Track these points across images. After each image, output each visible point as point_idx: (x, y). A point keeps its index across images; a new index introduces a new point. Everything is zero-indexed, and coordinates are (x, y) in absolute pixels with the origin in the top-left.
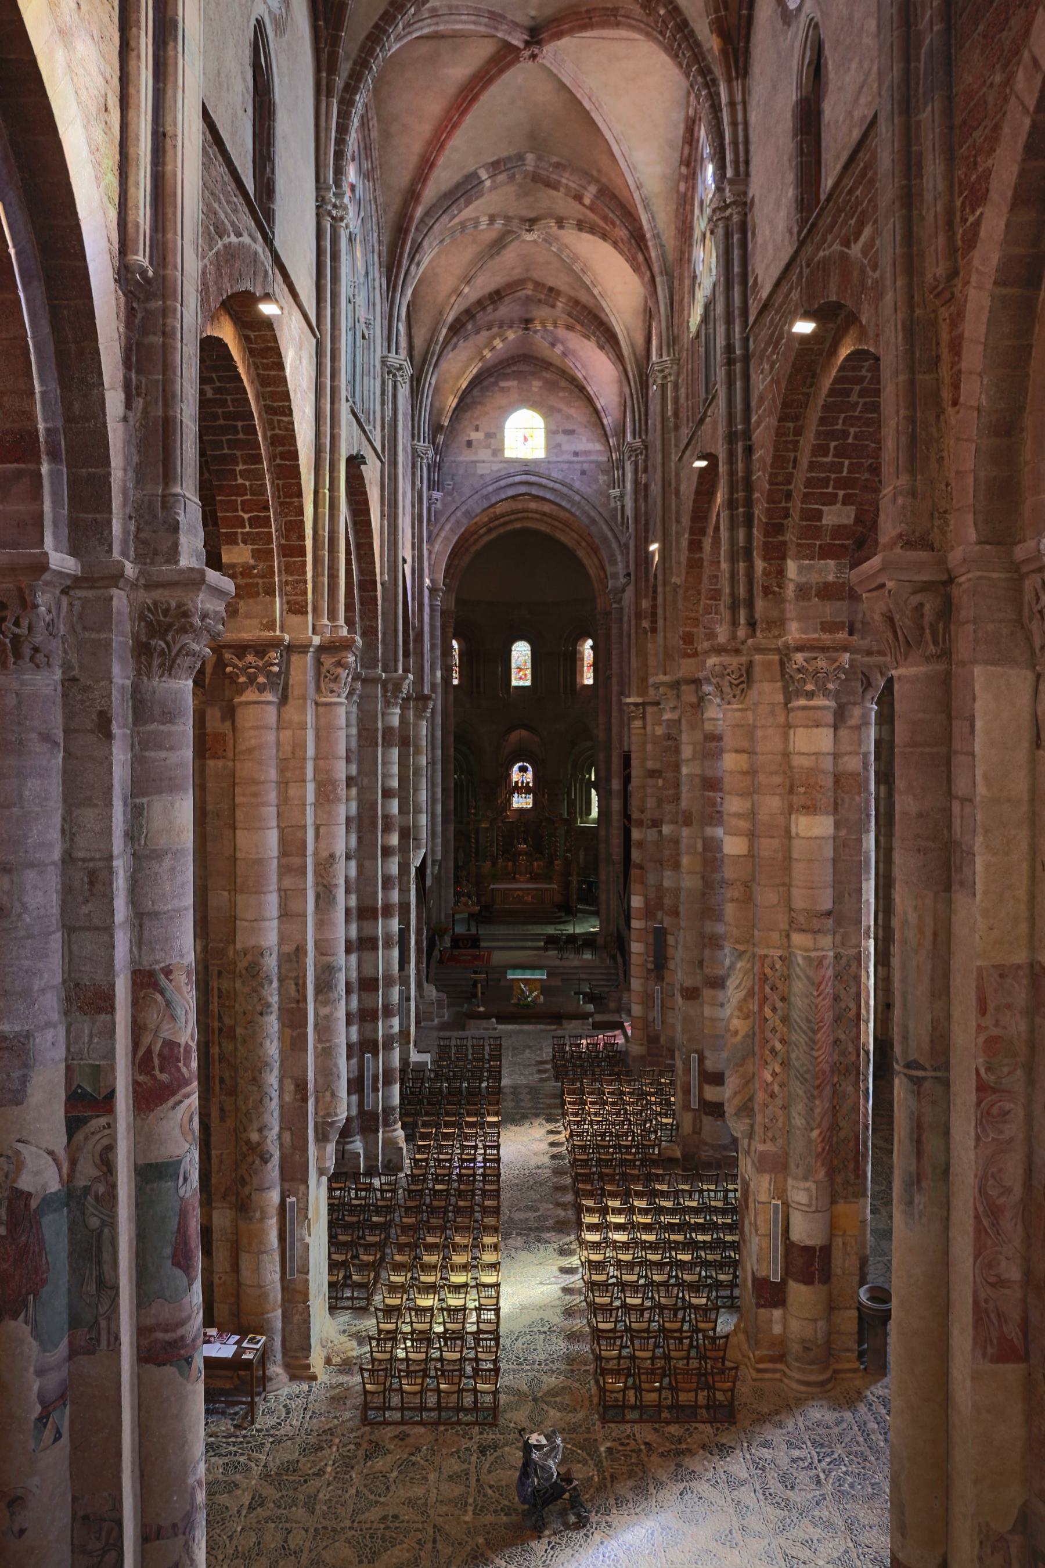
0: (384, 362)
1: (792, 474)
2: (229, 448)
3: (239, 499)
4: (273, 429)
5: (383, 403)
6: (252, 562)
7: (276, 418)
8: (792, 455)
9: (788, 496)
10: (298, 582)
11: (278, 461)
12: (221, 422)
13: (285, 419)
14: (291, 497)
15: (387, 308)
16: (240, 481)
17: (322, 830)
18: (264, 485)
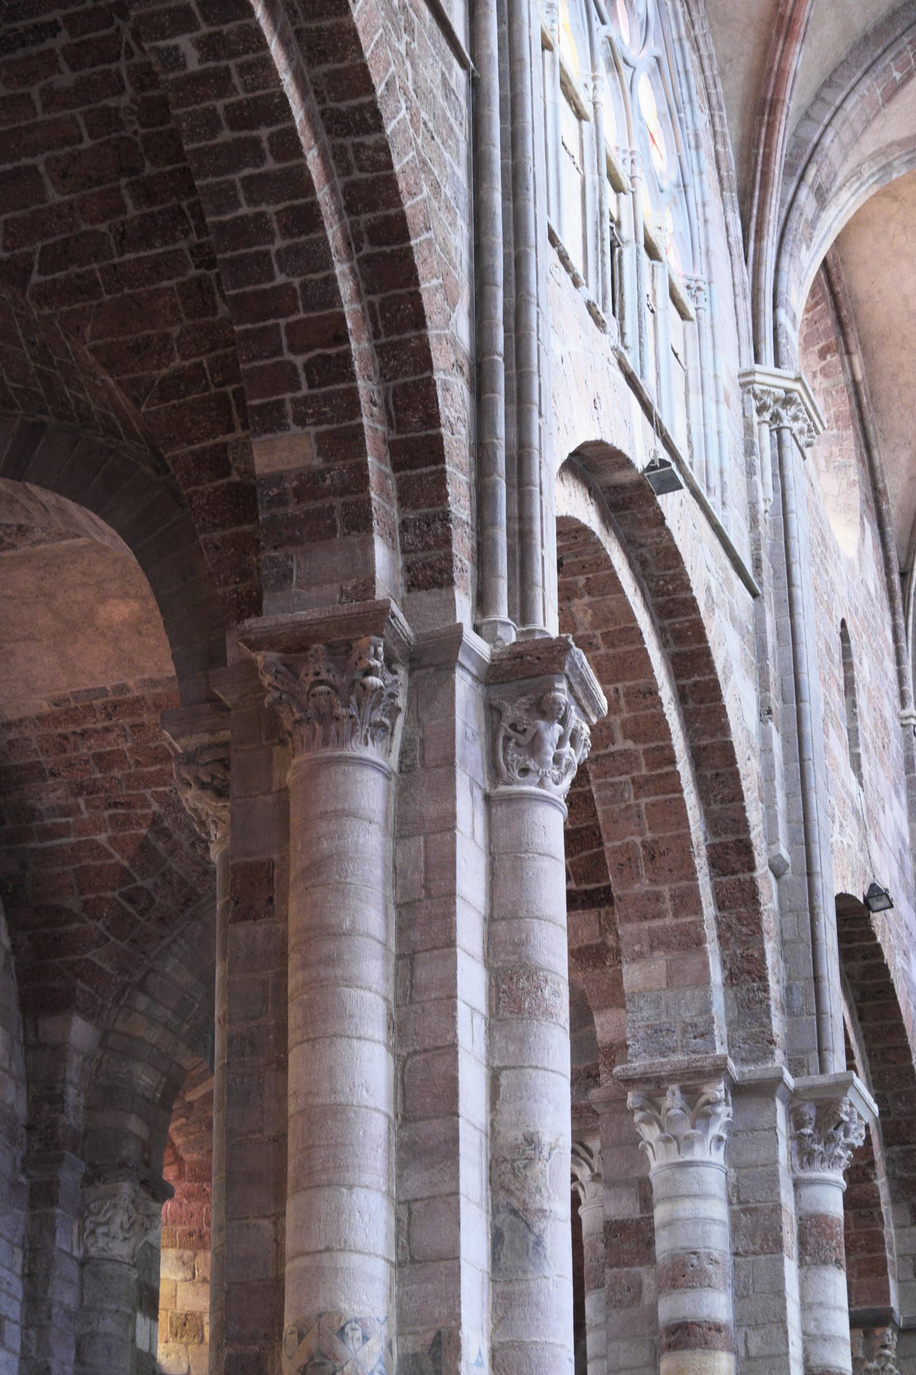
2: (251, 201)
3: (282, 322)
4: (347, 171)
5: (750, 471)
6: (317, 462)
7: (348, 141)
10: (429, 521)
11: (367, 249)
12: (226, 135)
13: (370, 140)
14: (400, 330)
15: (745, 276)
16: (280, 279)
17: (505, 1080)
18: (331, 280)
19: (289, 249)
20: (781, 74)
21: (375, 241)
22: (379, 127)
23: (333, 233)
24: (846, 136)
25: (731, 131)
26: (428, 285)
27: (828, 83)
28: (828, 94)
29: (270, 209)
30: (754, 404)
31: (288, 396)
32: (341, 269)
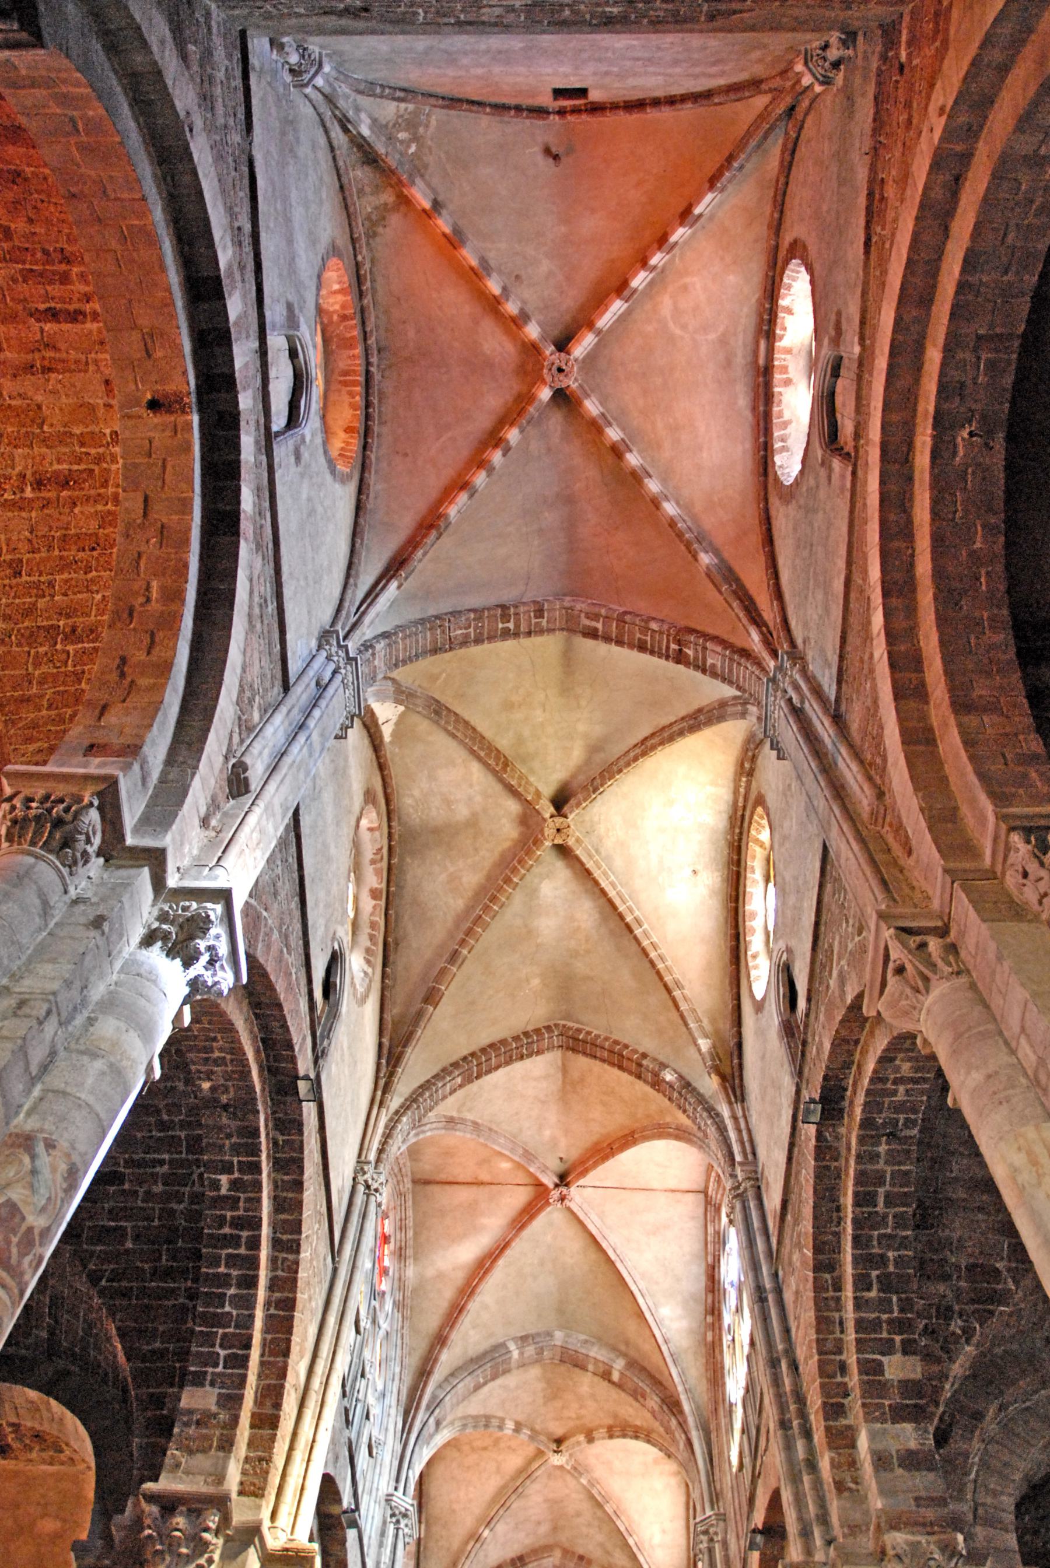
0: (389, 1498)
1: (841, 1340)
2: (227, 1266)
3: (221, 1331)
5: (381, 1545)
8: (837, 1315)
9: (843, 1368)
11: (272, 1311)
13: (291, 1257)
14: (276, 1355)
16: (227, 1309)
19: (235, 1295)
20: (436, 1360)
21: (276, 1308)
22: (298, 1252)
23: (261, 1294)
24: (455, 1400)
25: (408, 1380)
26: (295, 1339)
27: (452, 1375)
28: (451, 1379)
29: (235, 1273)
30: (389, 1512)
31: (210, 1370)
32: (259, 1314)
